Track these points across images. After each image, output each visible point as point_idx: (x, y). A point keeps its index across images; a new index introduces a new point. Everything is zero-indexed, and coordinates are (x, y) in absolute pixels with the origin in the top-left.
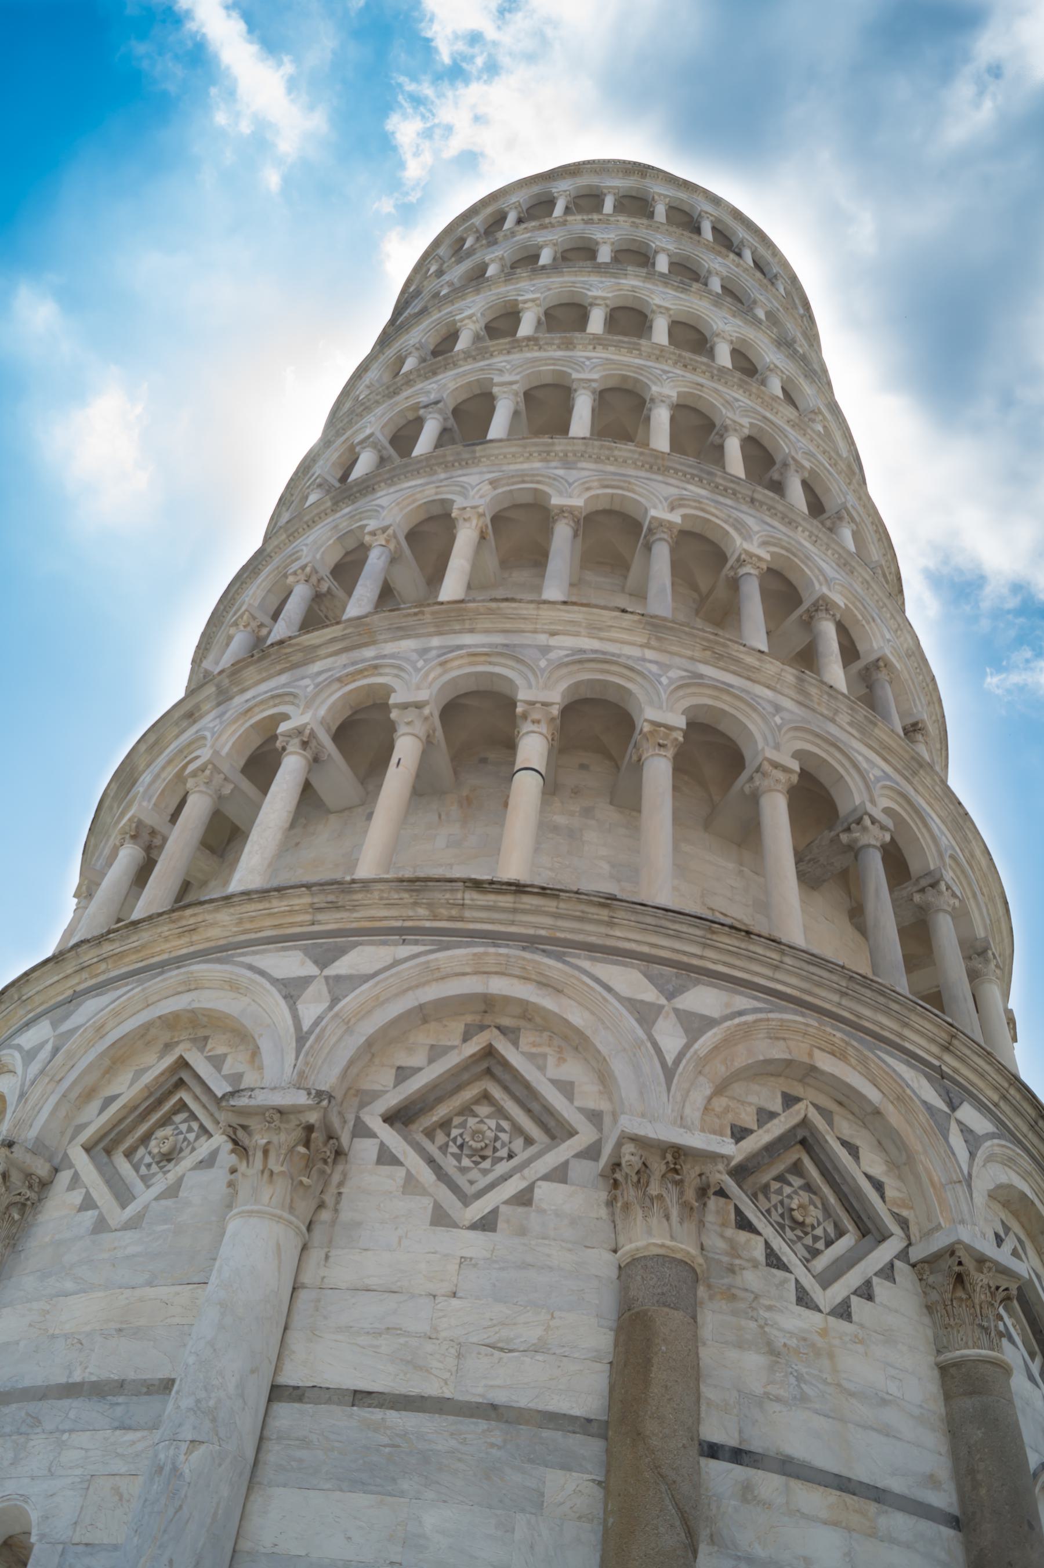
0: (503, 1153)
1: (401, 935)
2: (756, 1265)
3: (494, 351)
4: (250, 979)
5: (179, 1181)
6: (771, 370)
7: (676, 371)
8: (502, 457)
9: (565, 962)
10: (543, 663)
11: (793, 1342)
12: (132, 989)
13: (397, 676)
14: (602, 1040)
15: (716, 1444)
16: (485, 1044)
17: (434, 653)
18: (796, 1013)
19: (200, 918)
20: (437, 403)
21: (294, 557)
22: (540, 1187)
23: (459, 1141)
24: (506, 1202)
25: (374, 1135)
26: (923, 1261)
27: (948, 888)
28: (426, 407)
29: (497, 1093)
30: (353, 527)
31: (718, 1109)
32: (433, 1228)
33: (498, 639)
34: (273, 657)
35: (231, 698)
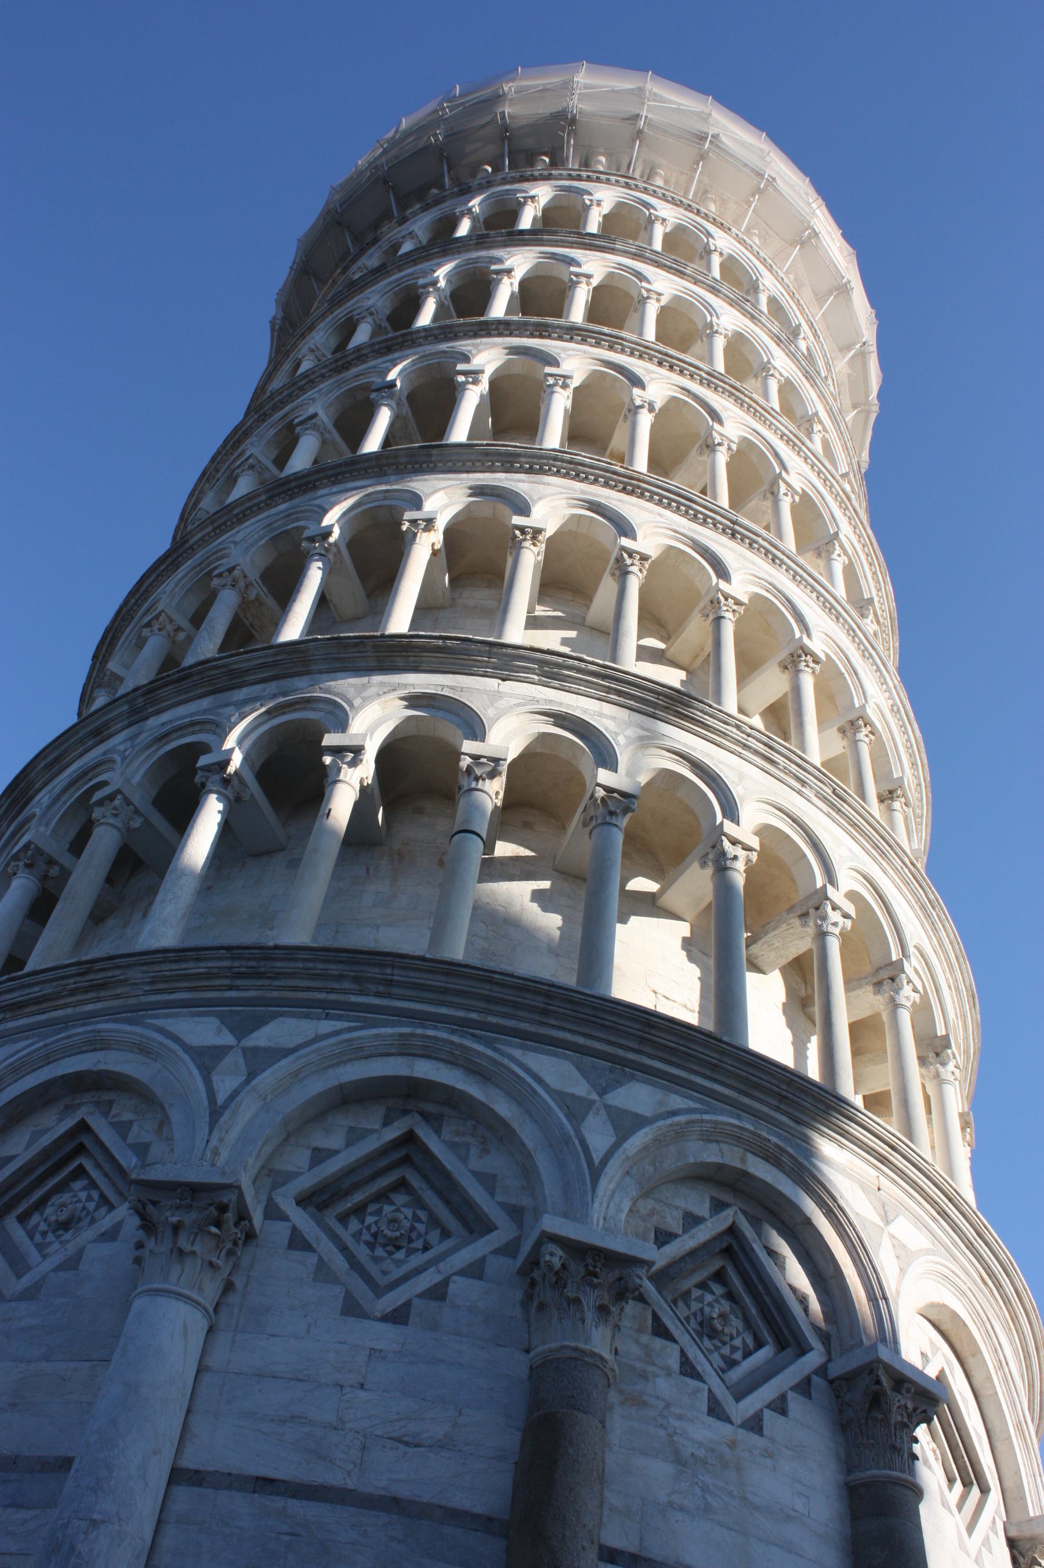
0: (419, 1244)
1: (324, 1009)
2: (669, 1373)
3: (459, 332)
4: (161, 1044)
5: (80, 1253)
8: (461, 464)
9: (495, 1049)
11: (701, 1453)
12: (33, 1044)
14: (528, 1134)
15: (616, 1550)
16: (405, 1130)
18: (731, 1115)
21: (220, 554)
22: (455, 1282)
23: (374, 1229)
24: (420, 1296)
25: (286, 1218)
26: (841, 1378)
27: (909, 981)
28: (378, 390)
29: (415, 1181)
30: (290, 527)
31: (643, 1211)
32: (344, 1317)
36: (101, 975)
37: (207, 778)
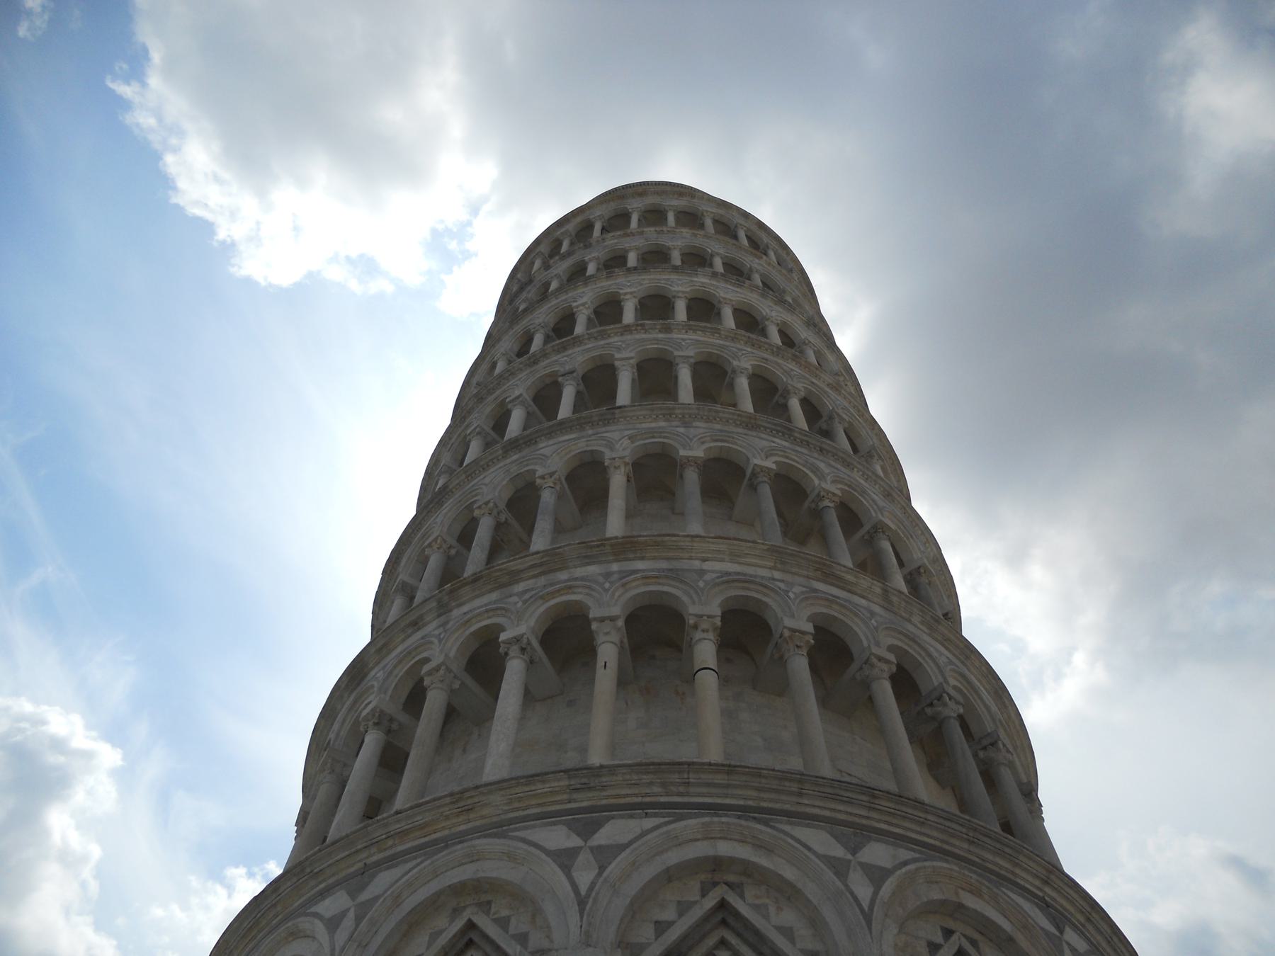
1: (643, 809)
6: (806, 344)
7: (745, 348)
9: (773, 828)
10: (701, 584)
12: (422, 862)
13: (587, 594)
16: (718, 899)
17: (616, 576)
19: (476, 800)
20: (572, 372)
21: (474, 493)
27: (1004, 745)
28: (563, 375)
33: (664, 565)
34: (484, 579)
35: (451, 610)
36: (469, 802)
37: (508, 649)
